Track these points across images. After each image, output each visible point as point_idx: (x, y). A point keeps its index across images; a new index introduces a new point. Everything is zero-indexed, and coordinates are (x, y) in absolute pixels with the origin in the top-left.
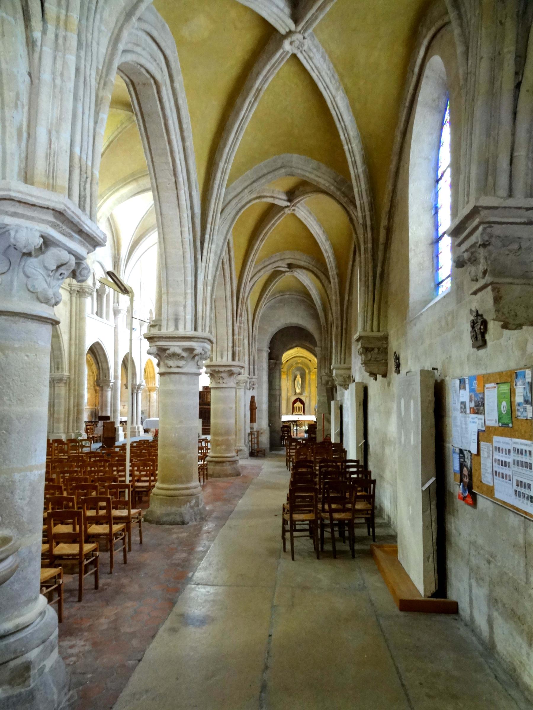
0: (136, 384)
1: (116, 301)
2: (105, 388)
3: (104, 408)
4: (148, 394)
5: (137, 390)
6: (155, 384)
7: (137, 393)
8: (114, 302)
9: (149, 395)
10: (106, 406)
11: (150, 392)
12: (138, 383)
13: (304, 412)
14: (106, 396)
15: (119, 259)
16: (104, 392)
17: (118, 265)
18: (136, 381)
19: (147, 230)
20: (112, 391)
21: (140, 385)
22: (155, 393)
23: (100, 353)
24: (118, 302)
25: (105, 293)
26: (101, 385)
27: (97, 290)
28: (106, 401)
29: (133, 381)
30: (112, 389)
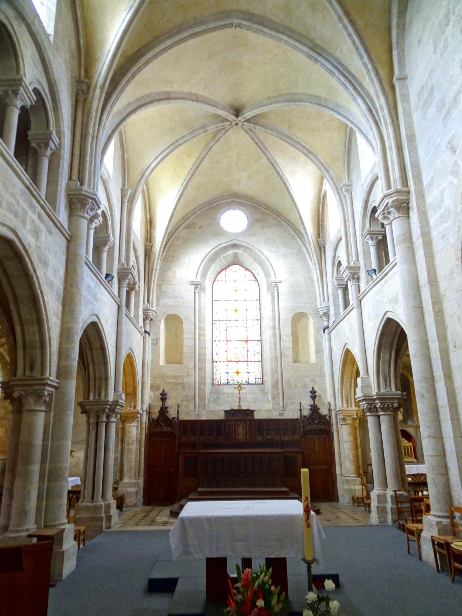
0: (106, 402)
1: (75, 176)
2: (30, 403)
3: (20, 468)
4: (120, 426)
5: (108, 416)
6: (135, 407)
7: (107, 424)
8: (70, 178)
9: (123, 429)
10: (28, 461)
11: (123, 422)
12: (111, 398)
13: (416, 457)
14: (31, 427)
15: (88, 87)
16: (25, 414)
17: (85, 100)
18: (106, 395)
19: (158, 37)
20: (47, 412)
21: (116, 403)
22: (135, 424)
23: (21, 292)
24: (81, 180)
25: (47, 145)
26: (16, 394)
27: (23, 108)
28: (30, 445)
29: (99, 395)
30: (48, 405)
